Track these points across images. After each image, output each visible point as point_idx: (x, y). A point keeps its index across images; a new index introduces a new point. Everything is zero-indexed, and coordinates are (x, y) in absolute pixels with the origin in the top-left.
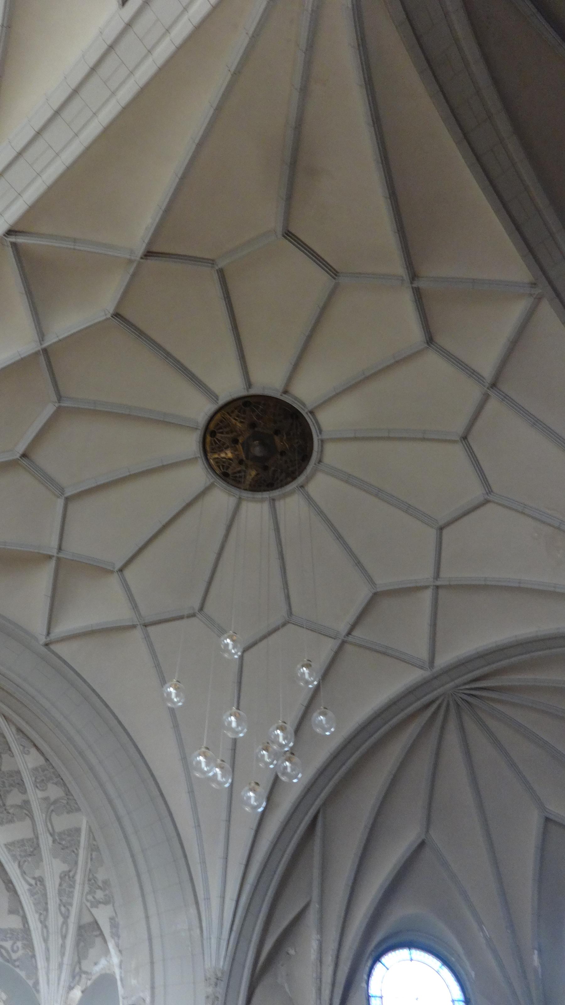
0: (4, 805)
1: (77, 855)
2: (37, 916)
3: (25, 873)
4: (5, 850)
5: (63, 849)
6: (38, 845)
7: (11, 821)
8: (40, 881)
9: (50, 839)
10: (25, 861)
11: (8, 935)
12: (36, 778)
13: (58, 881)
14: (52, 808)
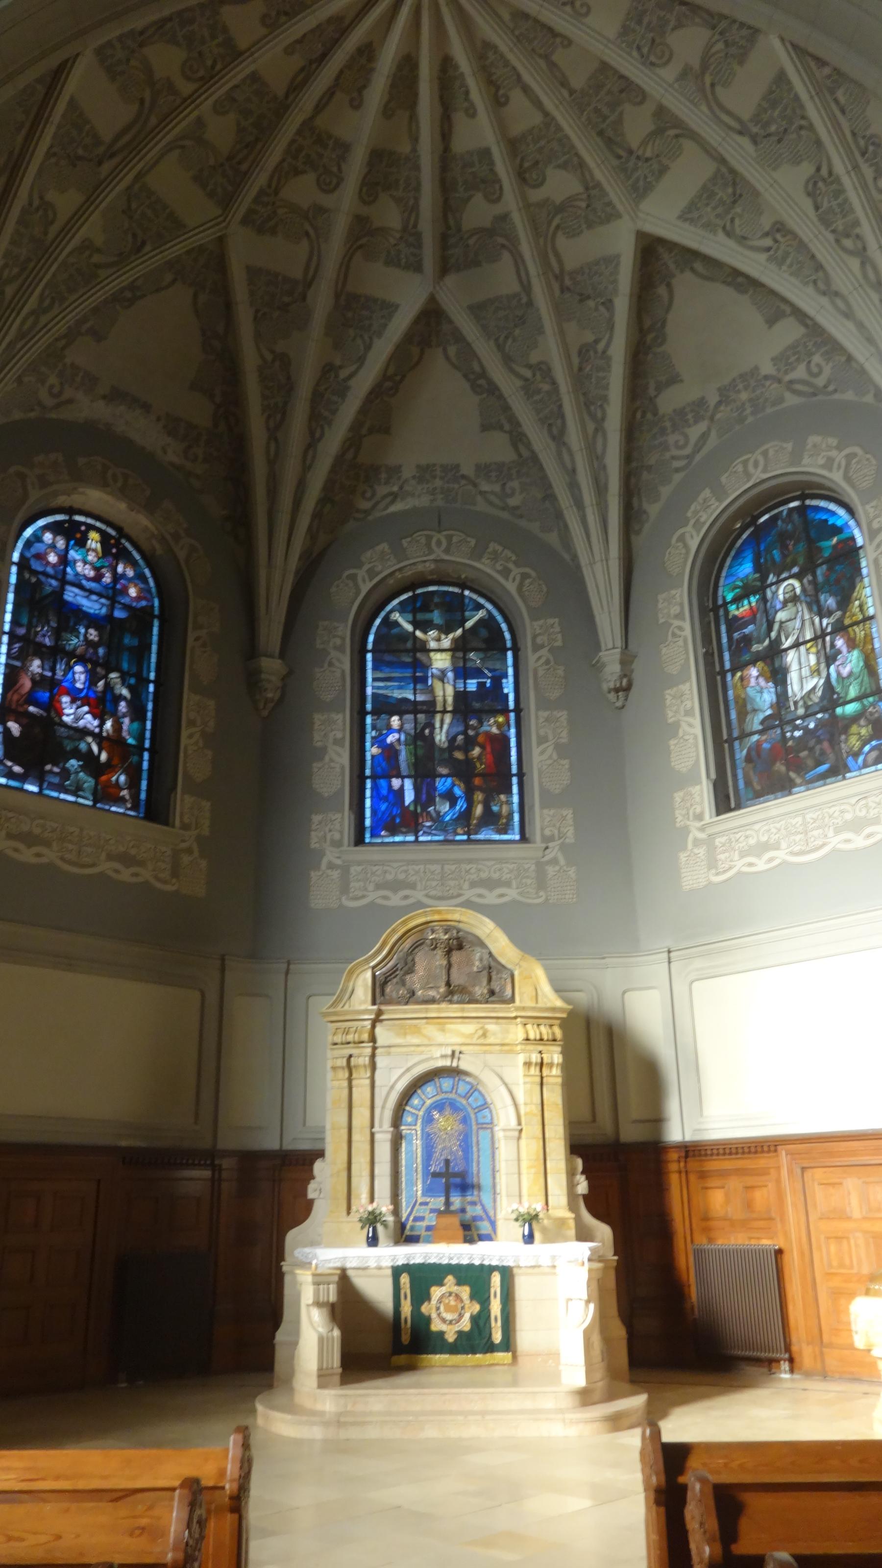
0: (631, 152)
1: (811, 127)
2: (810, 290)
3: (745, 238)
4: (686, 225)
5: (779, 141)
6: (732, 171)
7: (663, 170)
8: (778, 230)
9: (745, 142)
10: (732, 220)
11: (792, 359)
12: (639, 48)
13: (807, 204)
14: (708, 79)
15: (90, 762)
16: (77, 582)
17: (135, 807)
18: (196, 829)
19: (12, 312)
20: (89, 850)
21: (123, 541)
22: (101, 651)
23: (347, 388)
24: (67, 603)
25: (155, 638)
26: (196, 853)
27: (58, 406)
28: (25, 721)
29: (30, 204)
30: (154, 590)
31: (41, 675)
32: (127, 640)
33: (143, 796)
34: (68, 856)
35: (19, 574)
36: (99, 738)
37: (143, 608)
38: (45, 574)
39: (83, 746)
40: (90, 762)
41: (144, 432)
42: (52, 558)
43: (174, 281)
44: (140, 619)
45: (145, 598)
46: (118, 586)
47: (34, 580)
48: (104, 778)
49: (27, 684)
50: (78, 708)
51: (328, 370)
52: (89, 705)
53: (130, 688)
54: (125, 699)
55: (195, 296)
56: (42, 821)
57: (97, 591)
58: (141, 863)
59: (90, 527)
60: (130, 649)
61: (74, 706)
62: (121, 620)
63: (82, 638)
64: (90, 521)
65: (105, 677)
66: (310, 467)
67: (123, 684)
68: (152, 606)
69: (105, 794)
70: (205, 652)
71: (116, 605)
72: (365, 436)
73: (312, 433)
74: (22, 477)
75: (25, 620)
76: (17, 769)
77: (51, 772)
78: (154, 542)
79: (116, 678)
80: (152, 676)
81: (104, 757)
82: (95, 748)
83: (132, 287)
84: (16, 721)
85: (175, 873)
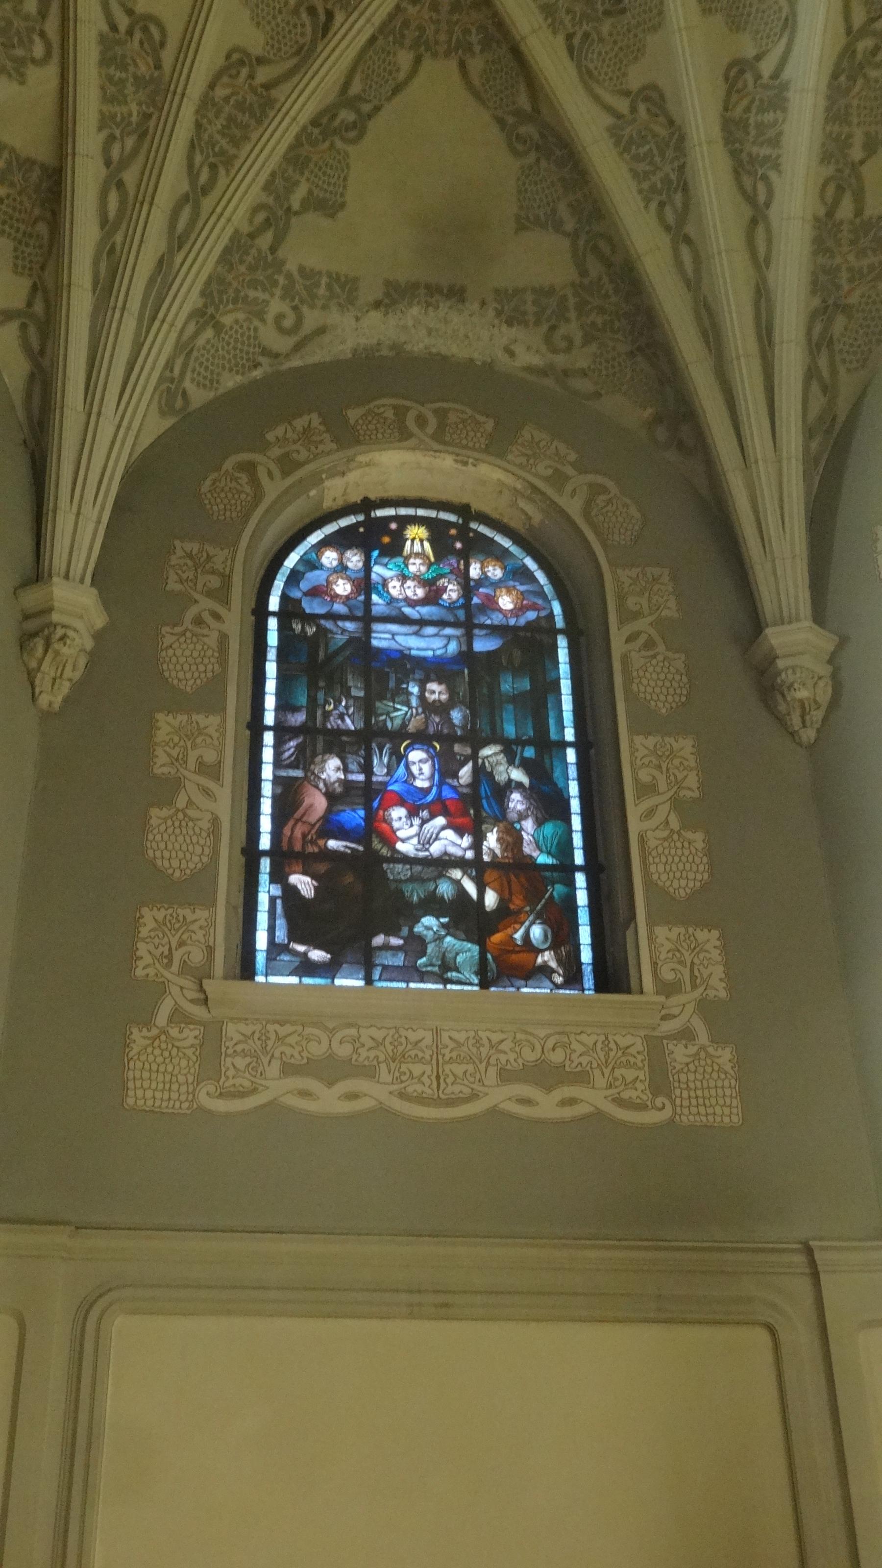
15: (465, 916)
16: (394, 613)
17: (573, 978)
18: (694, 986)
19: (142, 204)
20: (459, 1069)
21: (473, 525)
22: (456, 716)
23: (784, 87)
24: (380, 650)
25: (564, 669)
26: (703, 1037)
27: (298, 347)
28: (322, 868)
29: (114, 28)
30: (548, 589)
31: (347, 784)
32: (507, 685)
33: (586, 956)
34: (414, 1088)
35: (283, 629)
36: (477, 868)
37: (529, 624)
38: (332, 616)
39: (445, 889)
40: (465, 916)
41: (467, 335)
42: (342, 588)
43: (418, 61)
44: (529, 645)
45: (534, 607)
46: (476, 600)
47: (311, 631)
48: (497, 938)
49: (318, 803)
50: (424, 822)
51: (737, 74)
52: (445, 813)
53: (526, 765)
54: (519, 785)
55: (462, 65)
56: (353, 1031)
57: (435, 618)
58: (582, 1077)
59: (405, 522)
60: (515, 699)
61: (417, 822)
62: (489, 653)
63: (414, 702)
64: (403, 511)
65: (474, 757)
66: (768, 261)
67: (511, 762)
68: (551, 615)
69: (504, 968)
70: (654, 657)
71: (476, 631)
72: (862, 162)
73: (750, 199)
74: (249, 468)
75: (302, 700)
76: (317, 955)
77: (386, 947)
78: (522, 504)
79: (495, 754)
80: (569, 735)
81: (491, 899)
82: (471, 888)
83: (345, 98)
84: (305, 873)
85: (660, 1084)
